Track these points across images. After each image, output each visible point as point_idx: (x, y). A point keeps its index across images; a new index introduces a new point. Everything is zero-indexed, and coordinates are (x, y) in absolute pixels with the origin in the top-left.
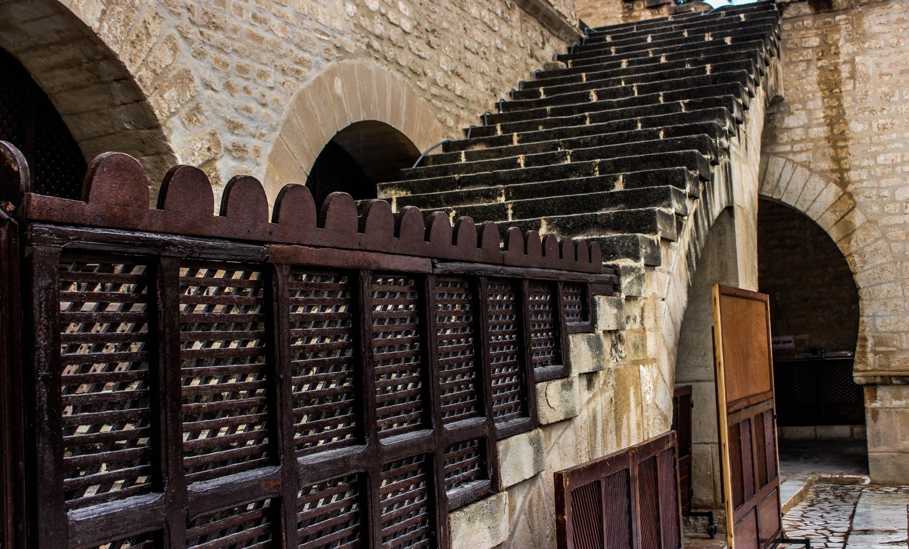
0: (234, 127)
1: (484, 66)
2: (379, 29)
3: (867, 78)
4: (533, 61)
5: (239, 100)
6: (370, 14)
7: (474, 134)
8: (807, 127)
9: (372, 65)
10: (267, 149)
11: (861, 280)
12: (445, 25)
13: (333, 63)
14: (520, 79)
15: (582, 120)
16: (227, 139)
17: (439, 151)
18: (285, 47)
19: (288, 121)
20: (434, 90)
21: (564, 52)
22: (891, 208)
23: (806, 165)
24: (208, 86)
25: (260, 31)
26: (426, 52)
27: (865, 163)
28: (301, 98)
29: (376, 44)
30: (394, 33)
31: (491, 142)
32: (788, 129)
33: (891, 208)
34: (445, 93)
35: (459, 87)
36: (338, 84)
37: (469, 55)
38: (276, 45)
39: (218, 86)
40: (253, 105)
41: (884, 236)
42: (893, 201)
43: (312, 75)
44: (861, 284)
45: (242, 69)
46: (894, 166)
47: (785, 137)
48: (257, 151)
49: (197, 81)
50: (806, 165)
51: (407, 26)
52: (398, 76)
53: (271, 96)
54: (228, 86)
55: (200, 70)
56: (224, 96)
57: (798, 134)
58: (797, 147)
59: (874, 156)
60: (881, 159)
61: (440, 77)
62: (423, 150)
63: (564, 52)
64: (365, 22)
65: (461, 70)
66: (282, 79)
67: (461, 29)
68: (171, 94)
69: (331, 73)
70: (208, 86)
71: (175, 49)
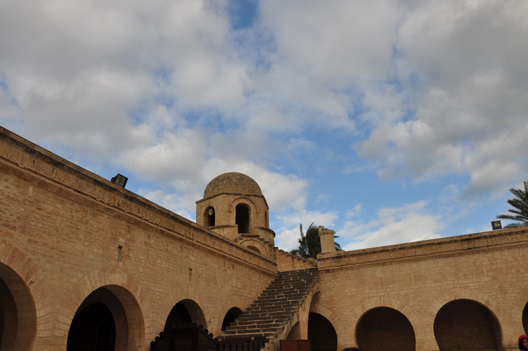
0: (213, 313)
2: (235, 289)
7: (252, 305)
8: (325, 298)
11: (337, 333)
15: (272, 304)
16: (213, 316)
17: (246, 311)
21: (273, 281)
22: (343, 316)
23: (325, 306)
30: (238, 289)
31: (256, 309)
33: (343, 316)
35: (250, 296)
46: (343, 307)
47: (320, 300)
50: (325, 306)
51: (240, 287)
59: (339, 305)
62: (242, 310)
63: (273, 281)
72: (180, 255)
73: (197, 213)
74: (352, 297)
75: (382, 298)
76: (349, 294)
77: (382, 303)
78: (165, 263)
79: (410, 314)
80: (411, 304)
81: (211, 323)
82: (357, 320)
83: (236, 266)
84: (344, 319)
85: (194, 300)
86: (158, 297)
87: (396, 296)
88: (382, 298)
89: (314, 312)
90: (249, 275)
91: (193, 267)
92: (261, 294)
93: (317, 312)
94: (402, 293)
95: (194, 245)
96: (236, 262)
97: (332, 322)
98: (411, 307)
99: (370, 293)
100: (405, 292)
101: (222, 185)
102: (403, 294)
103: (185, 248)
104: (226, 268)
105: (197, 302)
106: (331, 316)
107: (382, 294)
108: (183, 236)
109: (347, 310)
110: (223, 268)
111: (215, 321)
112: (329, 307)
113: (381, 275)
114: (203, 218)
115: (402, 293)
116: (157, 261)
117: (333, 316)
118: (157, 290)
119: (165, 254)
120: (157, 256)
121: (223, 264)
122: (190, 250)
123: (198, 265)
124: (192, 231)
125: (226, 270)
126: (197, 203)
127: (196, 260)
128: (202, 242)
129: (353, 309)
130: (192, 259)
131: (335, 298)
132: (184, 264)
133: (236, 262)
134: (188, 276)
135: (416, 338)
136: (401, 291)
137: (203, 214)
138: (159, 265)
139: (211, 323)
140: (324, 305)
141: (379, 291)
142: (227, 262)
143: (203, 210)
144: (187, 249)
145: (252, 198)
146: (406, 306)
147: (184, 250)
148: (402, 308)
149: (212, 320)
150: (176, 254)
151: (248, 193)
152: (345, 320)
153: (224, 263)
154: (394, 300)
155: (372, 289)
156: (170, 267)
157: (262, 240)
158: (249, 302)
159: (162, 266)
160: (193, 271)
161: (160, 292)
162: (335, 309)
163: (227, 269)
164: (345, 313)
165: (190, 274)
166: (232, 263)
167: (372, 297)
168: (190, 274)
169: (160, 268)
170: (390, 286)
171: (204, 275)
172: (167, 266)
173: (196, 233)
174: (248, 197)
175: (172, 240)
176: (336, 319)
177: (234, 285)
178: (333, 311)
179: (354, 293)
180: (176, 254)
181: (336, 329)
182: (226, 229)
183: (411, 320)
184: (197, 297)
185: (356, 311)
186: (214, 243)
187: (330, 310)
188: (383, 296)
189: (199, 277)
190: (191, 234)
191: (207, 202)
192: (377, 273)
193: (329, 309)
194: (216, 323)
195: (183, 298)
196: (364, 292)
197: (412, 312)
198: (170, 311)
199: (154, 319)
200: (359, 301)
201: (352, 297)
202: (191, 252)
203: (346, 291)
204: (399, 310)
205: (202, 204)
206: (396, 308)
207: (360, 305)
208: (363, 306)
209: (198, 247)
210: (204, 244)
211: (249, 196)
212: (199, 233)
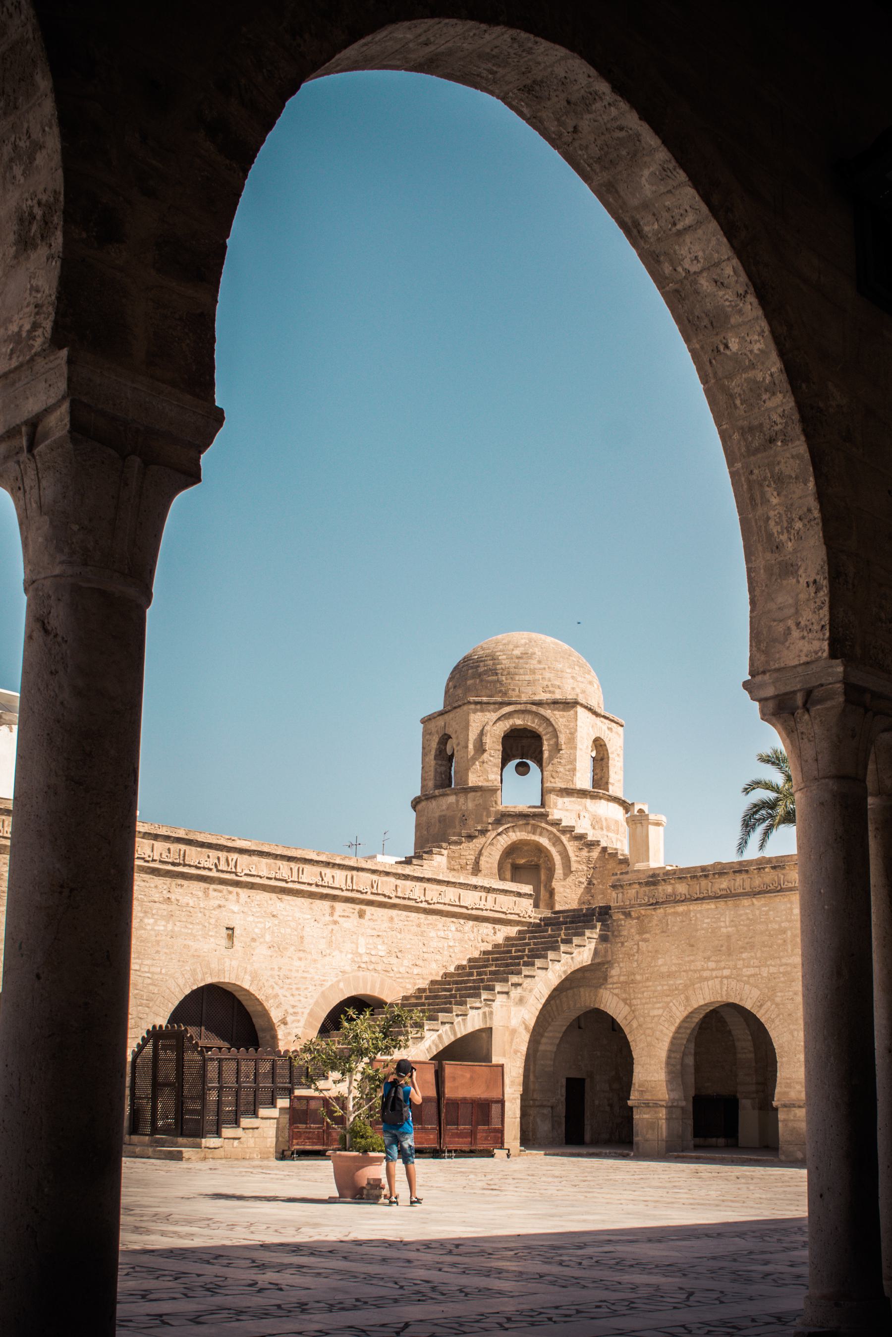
0: (293, 1007)
1: (438, 957)
3: (643, 953)
4: (485, 944)
5: (297, 998)
6: (360, 955)
8: (619, 975)
9: (361, 974)
10: (307, 1011)
12: (409, 946)
13: (340, 977)
14: (468, 957)
16: (291, 1011)
18: (317, 977)
19: (317, 1001)
20: (398, 976)
23: (617, 995)
24: (285, 996)
25: (305, 975)
26: (394, 960)
27: (640, 996)
28: (323, 993)
29: (363, 965)
30: (373, 959)
32: (611, 977)
34: (406, 975)
36: (341, 985)
37: (426, 955)
38: (312, 978)
39: (288, 995)
40: (302, 999)
41: (644, 1033)
42: (649, 1016)
43: (328, 984)
44: (635, 1056)
45: (298, 989)
47: (610, 980)
48: (303, 1013)
49: (281, 996)
50: (617, 995)
51: (382, 953)
52: (376, 975)
53: (309, 995)
54: (293, 995)
55: (281, 992)
56: (291, 998)
57: (615, 979)
58: (615, 986)
59: (643, 992)
60: (645, 994)
61: (402, 970)
64: (358, 959)
65: (419, 962)
66: (314, 988)
67: (421, 945)
68: (271, 1001)
69: (339, 981)
70: (285, 996)
71: (273, 988)
72: (202, 905)
73: (423, 748)
74: (668, 976)
75: (725, 981)
76: (664, 969)
77: (724, 993)
78: (163, 923)
79: (773, 1021)
80: (778, 1000)
81: (285, 1023)
82: (673, 1029)
83: (369, 910)
84: (650, 1026)
85: (238, 983)
86: (149, 981)
87: (752, 980)
88: (725, 981)
89: (596, 1006)
90: (419, 926)
91: (237, 923)
92: (458, 967)
93: (602, 1007)
94: (765, 972)
95: (237, 884)
96: (370, 903)
97: (626, 1030)
98: (777, 1005)
99: (704, 970)
100: (773, 970)
101: (473, 677)
102: (765, 975)
103: (215, 890)
104: (336, 917)
105: (246, 986)
106: (625, 1018)
107: (726, 972)
108: (210, 869)
109: (658, 1005)
110: (328, 918)
111: (299, 1021)
112: (624, 996)
113: (730, 929)
114: (433, 763)
115: (765, 972)
116: (146, 921)
117: (629, 1018)
118: (146, 969)
119: (164, 906)
120: (145, 912)
121: (328, 911)
122: (230, 892)
123: (251, 919)
124: (235, 856)
125: (335, 922)
126: (426, 721)
127: (246, 910)
128: (264, 873)
129: (668, 1003)
130: (235, 908)
131: (638, 977)
132: (213, 921)
133: (370, 903)
134: (224, 942)
135: (778, 1074)
136: (763, 969)
137: (433, 752)
138: (149, 927)
139: (285, 1023)
140: (616, 991)
141: (722, 964)
142: (340, 906)
143: (434, 745)
144: (220, 891)
145: (547, 712)
146: (769, 1003)
147: (212, 894)
148: (761, 1006)
149: (289, 1019)
150: (191, 904)
151: (537, 698)
152: (652, 1029)
153: (332, 907)
154: (747, 987)
155: (708, 959)
156: (176, 929)
157: (556, 823)
158: (415, 984)
159: (156, 928)
160: (237, 932)
161: (153, 973)
162: (634, 1002)
163: (339, 919)
164: (652, 1013)
165: (231, 937)
166: (358, 907)
167: (707, 979)
168: (231, 937)
169: (152, 933)
170: (744, 955)
171: (268, 938)
172: (170, 927)
173: (244, 859)
174: (534, 708)
175: (180, 881)
176: (635, 1024)
177: (362, 950)
178: (630, 1005)
179: (674, 968)
180: (191, 904)
181: (633, 1045)
182: (471, 795)
183: (773, 1034)
184: (248, 977)
185: (674, 1008)
186: (300, 872)
187: (626, 1003)
188: (727, 977)
189: (254, 940)
190: (232, 864)
191: (441, 722)
192: (722, 924)
193: (625, 1001)
194: (302, 1024)
195: (209, 981)
196: (692, 968)
197: (778, 1015)
198: (177, 1003)
199: (141, 1016)
200: (680, 987)
201: (668, 976)
202: (233, 897)
203: (660, 962)
204: (754, 1011)
205: (432, 725)
206: (748, 1007)
207: (682, 996)
208: (687, 999)
209: (252, 886)
210: (270, 879)
211: (539, 704)
212: (255, 859)
